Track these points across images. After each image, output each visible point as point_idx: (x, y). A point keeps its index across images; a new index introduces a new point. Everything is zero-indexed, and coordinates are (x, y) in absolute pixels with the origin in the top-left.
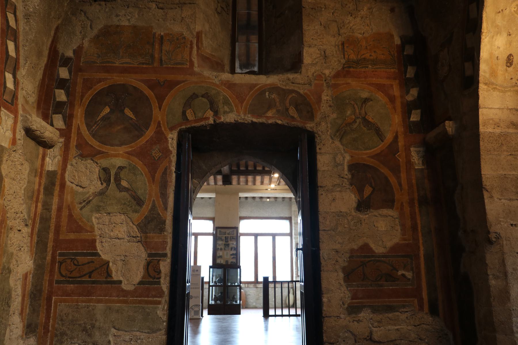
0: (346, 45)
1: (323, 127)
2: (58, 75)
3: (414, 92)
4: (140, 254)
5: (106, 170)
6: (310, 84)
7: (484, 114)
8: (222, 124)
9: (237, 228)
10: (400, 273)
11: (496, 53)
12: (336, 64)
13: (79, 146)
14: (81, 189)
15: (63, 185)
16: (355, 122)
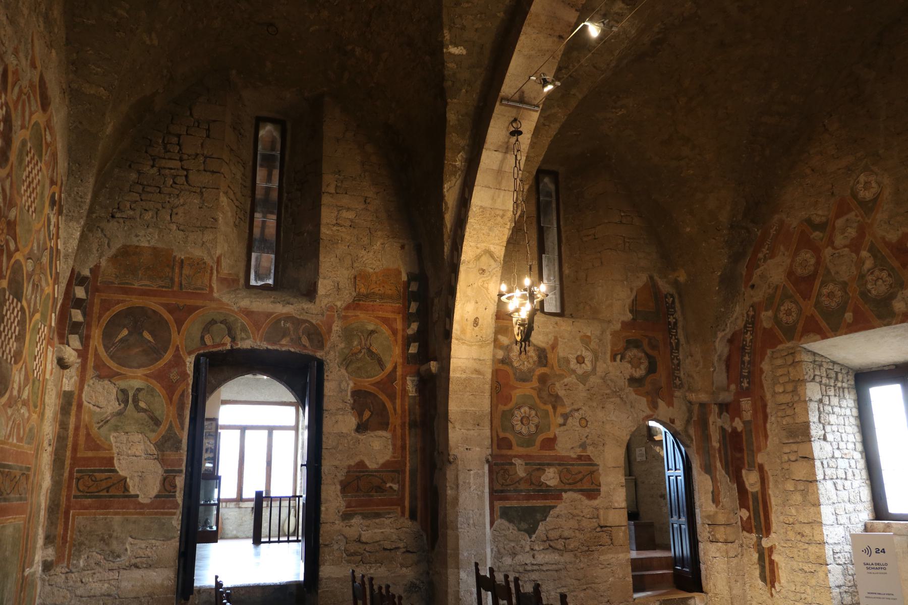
0: (358, 279)
1: (331, 357)
2: (74, 294)
3: (414, 326)
4: (155, 472)
5: (124, 392)
6: (322, 315)
7: (455, 363)
8: (239, 350)
10: (388, 485)
11: (466, 316)
12: (347, 296)
13: (96, 367)
14: (98, 409)
15: (80, 406)
16: (360, 352)
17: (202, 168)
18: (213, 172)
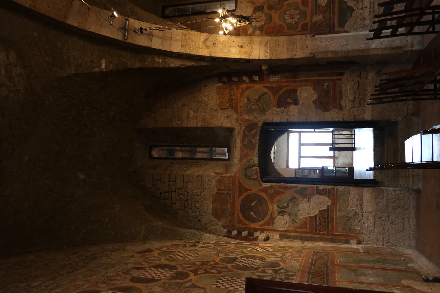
0: (222, 107)
1: (261, 119)
2: (235, 235)
3: (245, 78)
4: (317, 198)
5: (279, 213)
6: (241, 124)
7: (262, 57)
8: (259, 163)
9: (296, 170)
10: (325, 88)
11: (238, 52)
12: (231, 112)
13: (268, 225)
14: (288, 224)
15: (286, 231)
16: (258, 105)
17: (174, 183)
18: (176, 177)
